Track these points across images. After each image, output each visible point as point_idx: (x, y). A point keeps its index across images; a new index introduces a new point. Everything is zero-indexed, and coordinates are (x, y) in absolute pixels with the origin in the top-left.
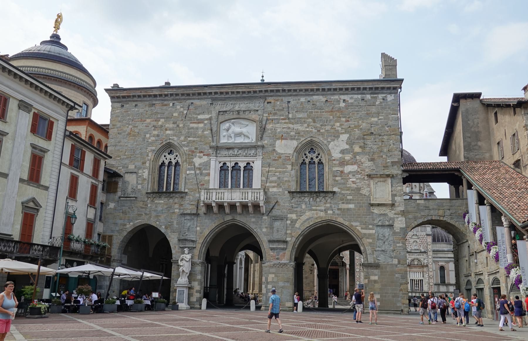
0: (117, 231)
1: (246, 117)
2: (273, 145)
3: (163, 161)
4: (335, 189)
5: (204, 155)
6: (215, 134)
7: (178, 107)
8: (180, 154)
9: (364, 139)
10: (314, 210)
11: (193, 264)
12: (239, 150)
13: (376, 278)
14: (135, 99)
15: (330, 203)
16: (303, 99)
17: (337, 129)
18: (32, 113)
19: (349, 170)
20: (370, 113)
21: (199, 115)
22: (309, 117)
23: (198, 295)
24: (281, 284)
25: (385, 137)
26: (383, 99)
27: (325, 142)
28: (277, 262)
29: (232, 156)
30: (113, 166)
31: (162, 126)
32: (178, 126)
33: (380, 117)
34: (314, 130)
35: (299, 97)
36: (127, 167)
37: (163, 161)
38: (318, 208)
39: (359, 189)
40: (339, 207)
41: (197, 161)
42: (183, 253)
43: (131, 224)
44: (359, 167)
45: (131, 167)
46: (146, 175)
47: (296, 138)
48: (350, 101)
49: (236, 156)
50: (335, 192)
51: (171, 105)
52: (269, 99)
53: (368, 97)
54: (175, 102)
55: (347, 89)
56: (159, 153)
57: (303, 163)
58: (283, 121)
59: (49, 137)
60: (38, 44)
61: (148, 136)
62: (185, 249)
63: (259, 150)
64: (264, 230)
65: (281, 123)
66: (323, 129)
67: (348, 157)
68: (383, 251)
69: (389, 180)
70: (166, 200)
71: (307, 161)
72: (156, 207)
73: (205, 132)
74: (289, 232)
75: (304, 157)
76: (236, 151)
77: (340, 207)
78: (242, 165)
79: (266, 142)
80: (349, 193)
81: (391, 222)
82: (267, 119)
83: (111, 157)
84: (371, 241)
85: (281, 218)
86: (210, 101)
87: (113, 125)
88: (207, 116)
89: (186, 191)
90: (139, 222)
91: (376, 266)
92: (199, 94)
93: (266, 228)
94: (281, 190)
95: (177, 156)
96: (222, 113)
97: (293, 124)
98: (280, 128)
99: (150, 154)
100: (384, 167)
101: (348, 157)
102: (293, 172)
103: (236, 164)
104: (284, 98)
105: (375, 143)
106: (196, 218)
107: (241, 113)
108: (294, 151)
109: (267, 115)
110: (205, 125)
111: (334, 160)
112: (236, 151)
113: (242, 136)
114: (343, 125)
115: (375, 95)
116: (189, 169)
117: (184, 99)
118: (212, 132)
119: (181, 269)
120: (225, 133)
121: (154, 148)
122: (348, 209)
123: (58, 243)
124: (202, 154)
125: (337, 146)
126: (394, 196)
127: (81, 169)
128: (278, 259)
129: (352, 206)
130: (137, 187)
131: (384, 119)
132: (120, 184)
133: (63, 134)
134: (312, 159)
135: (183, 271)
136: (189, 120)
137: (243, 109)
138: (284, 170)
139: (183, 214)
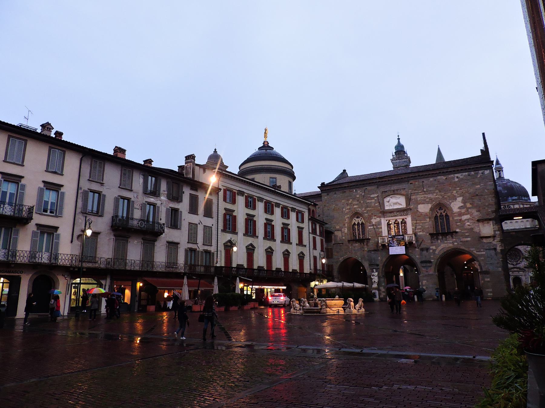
0: (335, 262)
1: (399, 193)
2: (417, 208)
3: (354, 222)
4: (458, 230)
5: (377, 217)
6: (382, 205)
7: (359, 192)
8: (363, 217)
9: (472, 199)
10: (445, 243)
11: (379, 278)
12: (397, 212)
13: (489, 279)
14: (334, 190)
15: (455, 238)
16: (431, 179)
17: (455, 194)
18: (296, 212)
19: (465, 219)
20: (474, 183)
21: (371, 195)
22: (436, 189)
23: (384, 294)
24: (431, 286)
25: (486, 196)
26: (482, 173)
27: (448, 203)
28: (427, 273)
29: (393, 217)
30: (328, 227)
31: (351, 203)
32: (360, 202)
33: (481, 185)
34: (440, 197)
35: (428, 178)
36: (336, 228)
37: (354, 222)
38: (448, 242)
39: (472, 229)
40: (461, 240)
41: (374, 221)
42: (374, 272)
43: (342, 258)
44: (471, 216)
45: (338, 227)
46: (346, 231)
47: (430, 202)
48: (461, 177)
49: (396, 216)
50: (458, 232)
51: (355, 191)
52: (411, 182)
53: (473, 173)
54: (357, 189)
55: (458, 170)
56: (351, 218)
57: (436, 217)
58: (421, 193)
59: (303, 222)
60: (257, 150)
61: (344, 209)
62: (374, 270)
63: (409, 211)
64: (417, 256)
65: (420, 194)
66: (445, 196)
67: (463, 211)
68: (491, 263)
69: (491, 222)
70: (359, 243)
71: (438, 215)
72: (354, 248)
73: (376, 204)
74: (432, 256)
75: (436, 212)
76: (395, 213)
77: (462, 240)
78: (400, 221)
79: (412, 206)
80: (467, 232)
81: (495, 247)
82: (411, 193)
83: (327, 224)
84: (483, 258)
85: (427, 249)
86: (376, 186)
87: (325, 206)
88: (376, 195)
89: (370, 238)
90: (346, 256)
91: (487, 273)
92: (370, 183)
93: (418, 255)
94: (424, 233)
95: (361, 219)
96: (384, 192)
97: (427, 194)
98: (420, 197)
99: (347, 220)
100: (487, 214)
101: (463, 211)
102: (431, 223)
103: (396, 220)
104: (420, 180)
105: (480, 201)
106: (377, 252)
107: (396, 191)
108: (430, 210)
109: (411, 191)
110: (375, 200)
111: (455, 213)
112: (395, 213)
113: (398, 204)
114: (458, 192)
115: (477, 172)
116: (370, 226)
117: (361, 187)
118: (380, 204)
119: (373, 280)
120: (388, 204)
121: (349, 216)
122: (467, 241)
123: (313, 271)
124: (376, 217)
125: (456, 205)
126: (494, 231)
127: (316, 234)
128: (427, 272)
129: (469, 239)
130: (342, 238)
131: (484, 185)
132: (333, 237)
133: (308, 218)
134: (441, 213)
135: (374, 281)
136: (366, 198)
137: (396, 189)
138: (425, 221)
139: (369, 251)
